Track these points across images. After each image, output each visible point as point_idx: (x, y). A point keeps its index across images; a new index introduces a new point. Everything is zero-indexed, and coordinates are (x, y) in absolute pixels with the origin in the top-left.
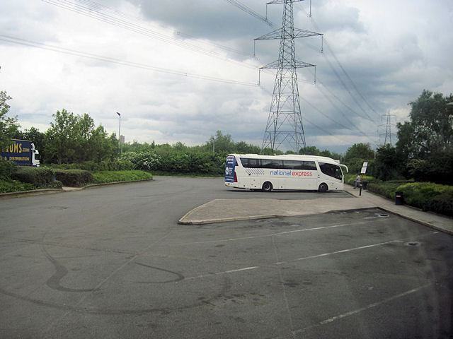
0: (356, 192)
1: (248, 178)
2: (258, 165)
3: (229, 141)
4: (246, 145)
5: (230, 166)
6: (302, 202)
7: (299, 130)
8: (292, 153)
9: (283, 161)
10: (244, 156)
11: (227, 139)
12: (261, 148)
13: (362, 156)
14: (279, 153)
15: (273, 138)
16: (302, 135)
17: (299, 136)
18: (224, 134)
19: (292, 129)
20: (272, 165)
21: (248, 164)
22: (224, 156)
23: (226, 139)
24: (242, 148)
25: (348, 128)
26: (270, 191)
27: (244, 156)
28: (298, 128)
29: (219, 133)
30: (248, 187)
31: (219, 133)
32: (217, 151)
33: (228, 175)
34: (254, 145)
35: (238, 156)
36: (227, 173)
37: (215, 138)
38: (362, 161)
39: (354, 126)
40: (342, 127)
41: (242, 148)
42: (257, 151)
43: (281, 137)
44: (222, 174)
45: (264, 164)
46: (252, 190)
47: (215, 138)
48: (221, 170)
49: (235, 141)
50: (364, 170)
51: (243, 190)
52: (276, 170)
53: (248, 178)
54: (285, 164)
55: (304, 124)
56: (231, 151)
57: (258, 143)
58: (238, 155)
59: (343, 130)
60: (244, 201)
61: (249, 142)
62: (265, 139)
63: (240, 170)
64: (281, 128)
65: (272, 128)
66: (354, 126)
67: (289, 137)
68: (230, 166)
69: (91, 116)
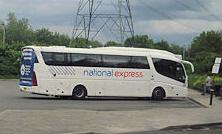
0: (205, 100)
1: (53, 80)
2: (67, 61)
3: (25, 27)
4: (49, 33)
5: (27, 63)
6: (129, 114)
7: (125, 12)
8: (114, 44)
9: (101, 55)
10: (46, 49)
11: (22, 25)
12: (71, 37)
13: (213, 49)
14: (96, 45)
15: (87, 22)
16: (129, 20)
17: (124, 20)
18: (18, 18)
19: (115, 11)
20: (86, 62)
21: (52, 60)
22: (19, 49)
23: (20, 24)
24: (44, 38)
25: (193, 10)
26: (83, 99)
27: (46, 49)
28: (123, 10)
29: (11, 16)
30: (53, 92)
31: (11, 16)
32: (8, 41)
33: (25, 76)
34: (61, 34)
35: (38, 49)
36: (22, 73)
37: (6, 23)
38: (213, 57)
39: (203, 6)
40: (186, 7)
41: (44, 38)
42: (65, 42)
43: (100, 22)
44: (16, 74)
45: (76, 60)
46: (58, 98)
47: (6, 23)
48: (13, 68)
49: (35, 27)
50: (216, 69)
51: (46, 98)
52: (92, 69)
53: (53, 80)
54: (105, 61)
55: (131, 3)
56: (29, 42)
57: (66, 31)
58: (39, 47)
59: (188, 12)
60: (46, 112)
61: (53, 30)
62: (76, 25)
63: (41, 68)
64: (98, 9)
65: (86, 10)
66: (203, 6)
67: (111, 22)
68: (27, 63)
69: (12, 12)
